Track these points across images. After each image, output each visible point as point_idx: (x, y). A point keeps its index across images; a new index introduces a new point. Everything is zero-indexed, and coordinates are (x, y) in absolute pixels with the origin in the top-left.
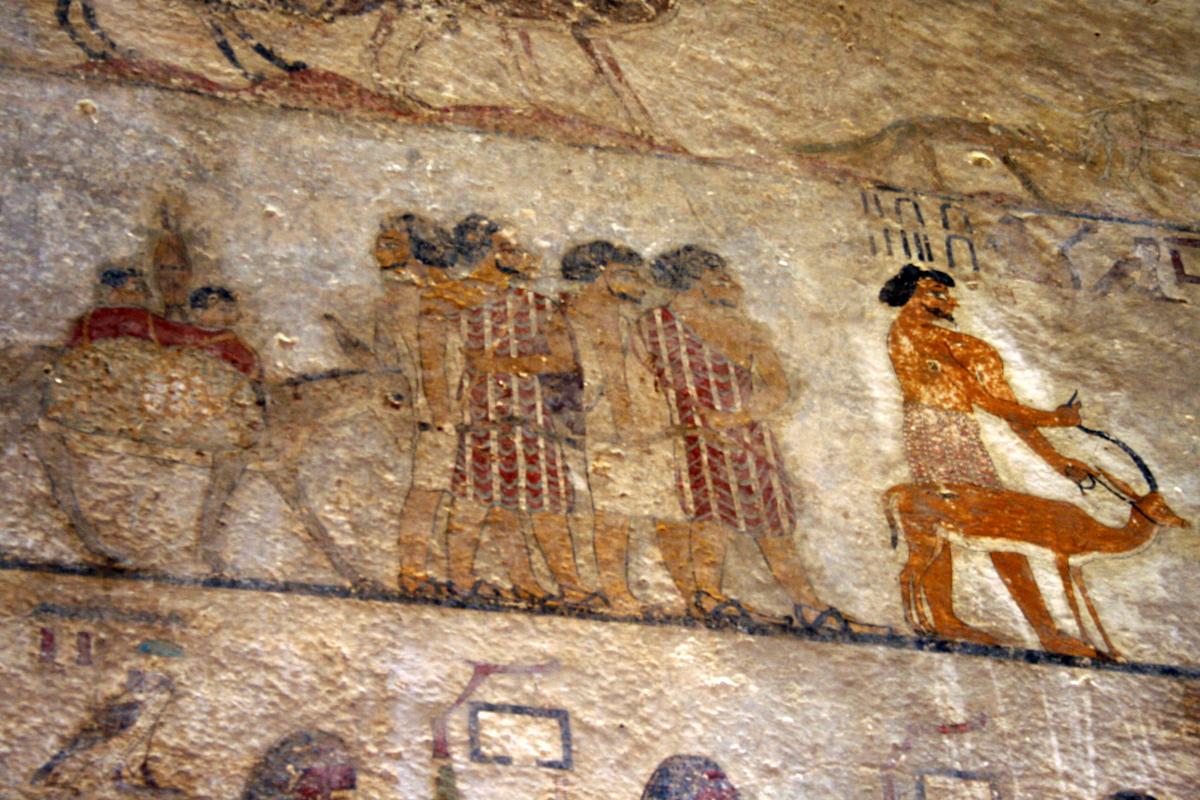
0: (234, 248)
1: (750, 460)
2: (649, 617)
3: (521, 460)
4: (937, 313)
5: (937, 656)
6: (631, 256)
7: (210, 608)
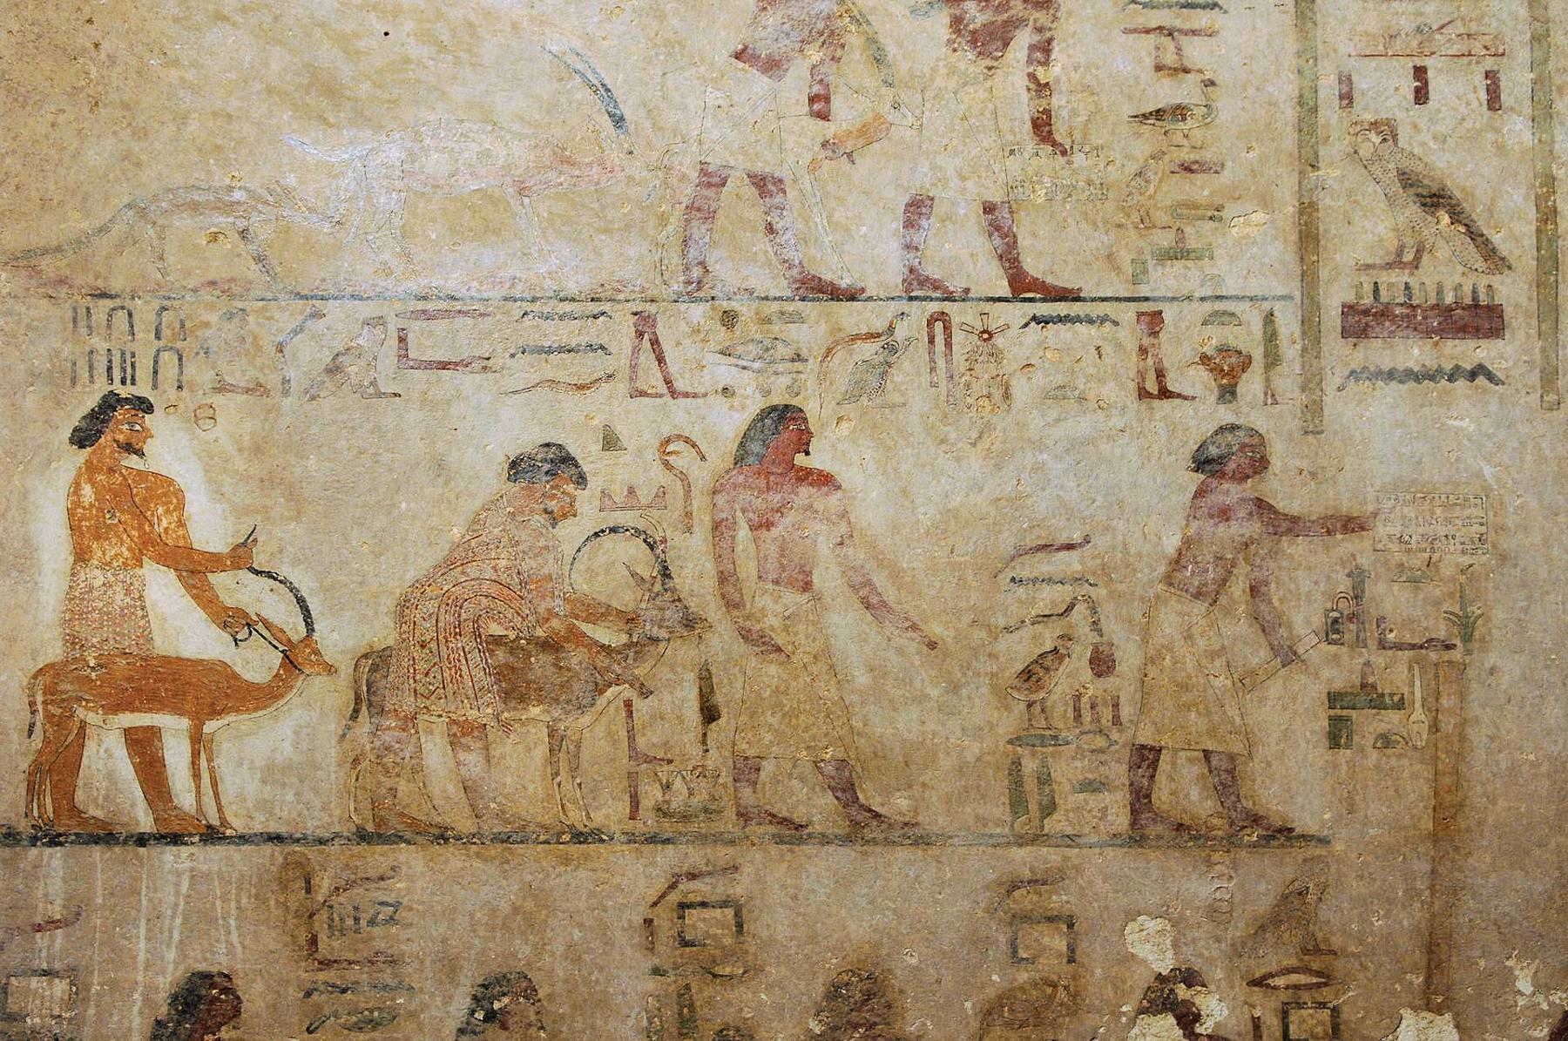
4: (129, 448)
5: (48, 851)
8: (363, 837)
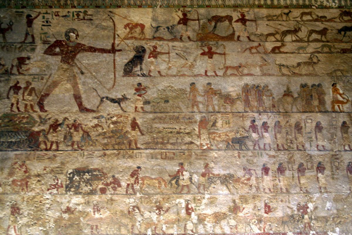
2: (317, 112)
6: (315, 85)
7: (292, 114)
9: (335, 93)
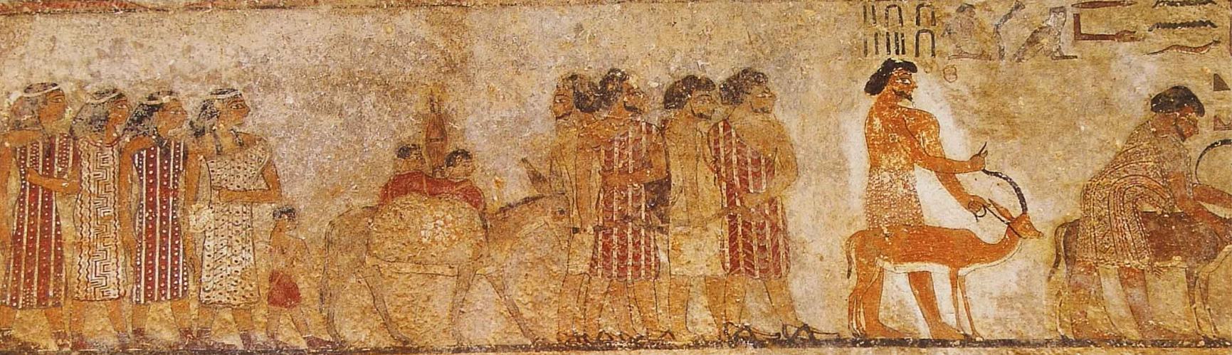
0: (471, 119)
1: (767, 227)
3: (630, 246)
4: (902, 95)
5: (864, 349)
6: (709, 84)
8: (1064, 342)
9: (897, 159)
